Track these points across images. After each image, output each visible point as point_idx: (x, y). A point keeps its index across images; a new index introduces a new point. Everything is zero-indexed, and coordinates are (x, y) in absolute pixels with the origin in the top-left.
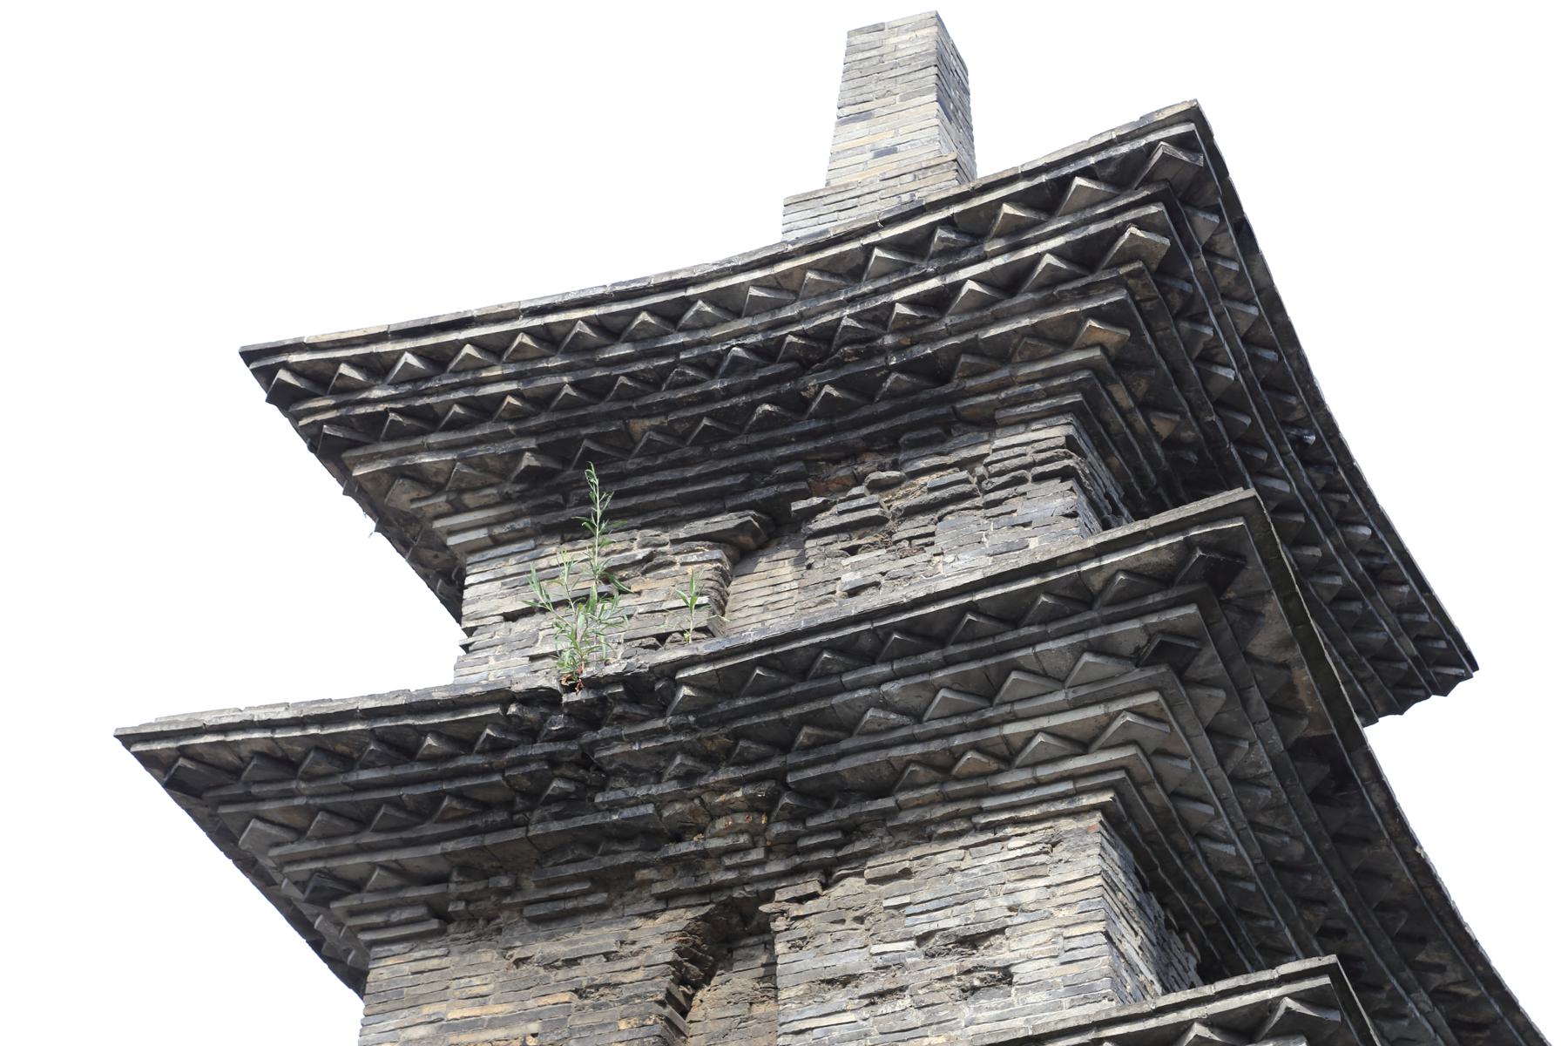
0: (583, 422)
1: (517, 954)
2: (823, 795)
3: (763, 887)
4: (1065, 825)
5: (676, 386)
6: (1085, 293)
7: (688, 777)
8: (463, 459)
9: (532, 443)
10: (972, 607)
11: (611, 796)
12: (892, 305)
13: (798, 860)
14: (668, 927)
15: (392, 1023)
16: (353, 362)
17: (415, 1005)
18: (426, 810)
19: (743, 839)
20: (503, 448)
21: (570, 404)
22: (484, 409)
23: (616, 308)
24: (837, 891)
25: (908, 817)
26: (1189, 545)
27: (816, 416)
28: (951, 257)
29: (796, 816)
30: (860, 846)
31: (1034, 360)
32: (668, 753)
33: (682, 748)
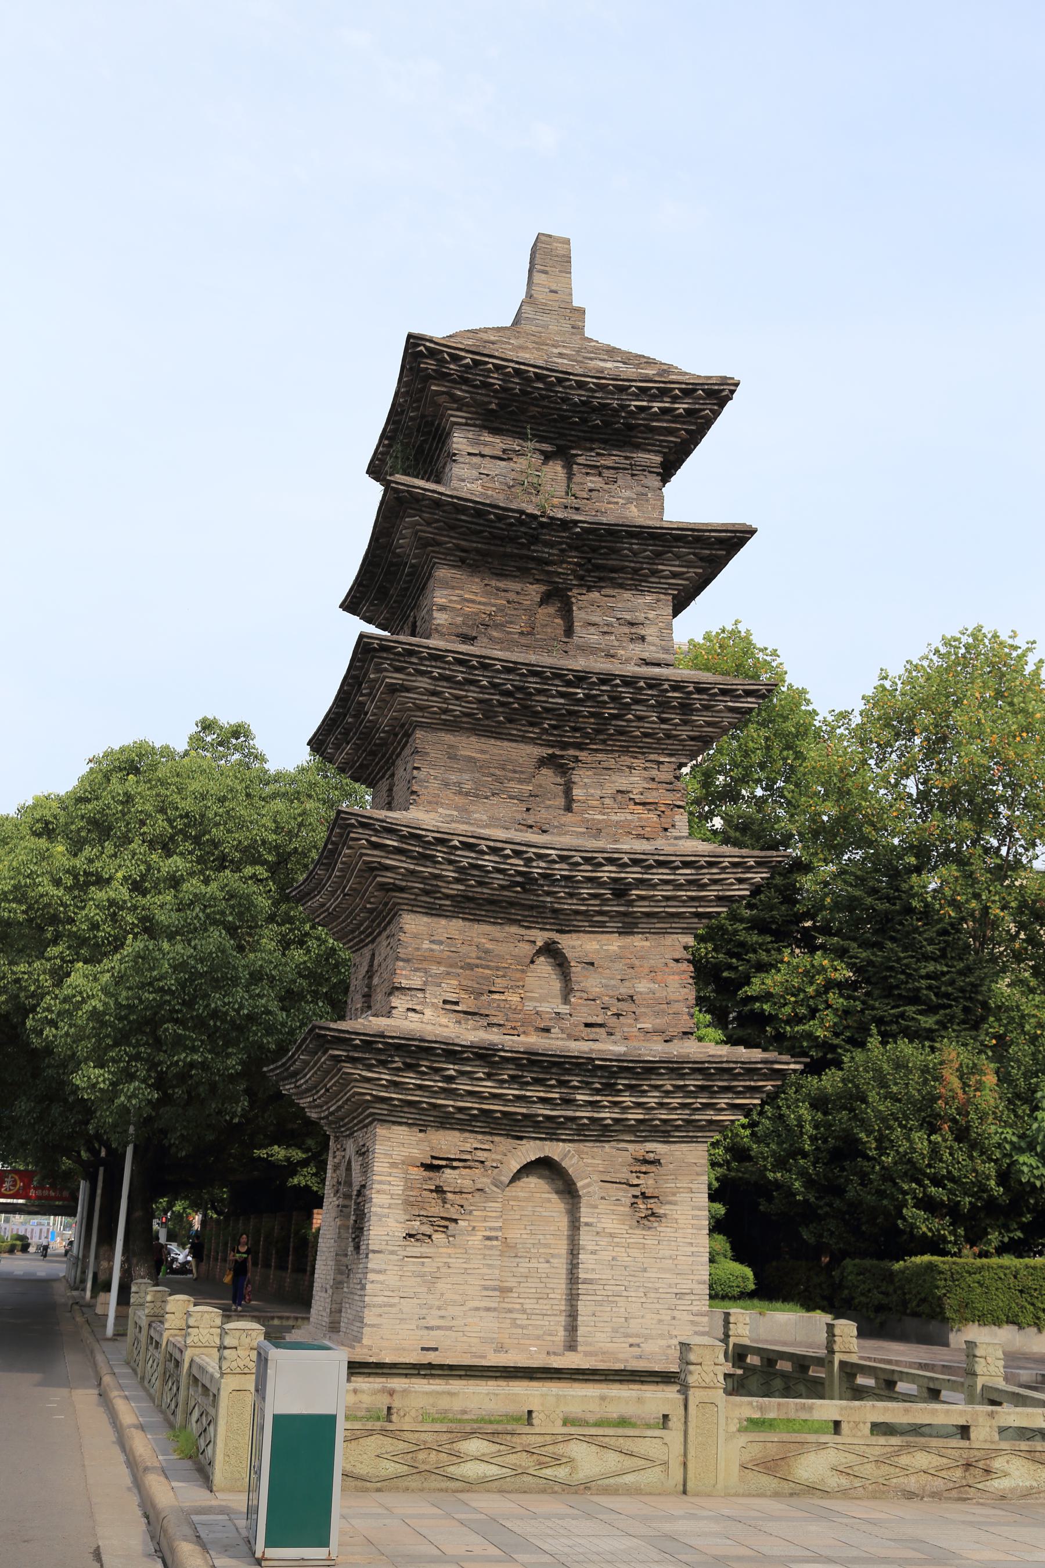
1: (486, 582)
2: (598, 568)
4: (662, 596)
5: (551, 402)
6: (684, 423)
7: (562, 551)
8: (471, 398)
11: (536, 548)
12: (630, 405)
15: (445, 592)
16: (449, 354)
17: (453, 588)
20: (486, 399)
21: (516, 395)
22: (486, 385)
23: (545, 372)
25: (620, 581)
26: (733, 537)
28: (653, 398)
29: (588, 571)
31: (660, 435)
32: (561, 543)
33: (566, 543)
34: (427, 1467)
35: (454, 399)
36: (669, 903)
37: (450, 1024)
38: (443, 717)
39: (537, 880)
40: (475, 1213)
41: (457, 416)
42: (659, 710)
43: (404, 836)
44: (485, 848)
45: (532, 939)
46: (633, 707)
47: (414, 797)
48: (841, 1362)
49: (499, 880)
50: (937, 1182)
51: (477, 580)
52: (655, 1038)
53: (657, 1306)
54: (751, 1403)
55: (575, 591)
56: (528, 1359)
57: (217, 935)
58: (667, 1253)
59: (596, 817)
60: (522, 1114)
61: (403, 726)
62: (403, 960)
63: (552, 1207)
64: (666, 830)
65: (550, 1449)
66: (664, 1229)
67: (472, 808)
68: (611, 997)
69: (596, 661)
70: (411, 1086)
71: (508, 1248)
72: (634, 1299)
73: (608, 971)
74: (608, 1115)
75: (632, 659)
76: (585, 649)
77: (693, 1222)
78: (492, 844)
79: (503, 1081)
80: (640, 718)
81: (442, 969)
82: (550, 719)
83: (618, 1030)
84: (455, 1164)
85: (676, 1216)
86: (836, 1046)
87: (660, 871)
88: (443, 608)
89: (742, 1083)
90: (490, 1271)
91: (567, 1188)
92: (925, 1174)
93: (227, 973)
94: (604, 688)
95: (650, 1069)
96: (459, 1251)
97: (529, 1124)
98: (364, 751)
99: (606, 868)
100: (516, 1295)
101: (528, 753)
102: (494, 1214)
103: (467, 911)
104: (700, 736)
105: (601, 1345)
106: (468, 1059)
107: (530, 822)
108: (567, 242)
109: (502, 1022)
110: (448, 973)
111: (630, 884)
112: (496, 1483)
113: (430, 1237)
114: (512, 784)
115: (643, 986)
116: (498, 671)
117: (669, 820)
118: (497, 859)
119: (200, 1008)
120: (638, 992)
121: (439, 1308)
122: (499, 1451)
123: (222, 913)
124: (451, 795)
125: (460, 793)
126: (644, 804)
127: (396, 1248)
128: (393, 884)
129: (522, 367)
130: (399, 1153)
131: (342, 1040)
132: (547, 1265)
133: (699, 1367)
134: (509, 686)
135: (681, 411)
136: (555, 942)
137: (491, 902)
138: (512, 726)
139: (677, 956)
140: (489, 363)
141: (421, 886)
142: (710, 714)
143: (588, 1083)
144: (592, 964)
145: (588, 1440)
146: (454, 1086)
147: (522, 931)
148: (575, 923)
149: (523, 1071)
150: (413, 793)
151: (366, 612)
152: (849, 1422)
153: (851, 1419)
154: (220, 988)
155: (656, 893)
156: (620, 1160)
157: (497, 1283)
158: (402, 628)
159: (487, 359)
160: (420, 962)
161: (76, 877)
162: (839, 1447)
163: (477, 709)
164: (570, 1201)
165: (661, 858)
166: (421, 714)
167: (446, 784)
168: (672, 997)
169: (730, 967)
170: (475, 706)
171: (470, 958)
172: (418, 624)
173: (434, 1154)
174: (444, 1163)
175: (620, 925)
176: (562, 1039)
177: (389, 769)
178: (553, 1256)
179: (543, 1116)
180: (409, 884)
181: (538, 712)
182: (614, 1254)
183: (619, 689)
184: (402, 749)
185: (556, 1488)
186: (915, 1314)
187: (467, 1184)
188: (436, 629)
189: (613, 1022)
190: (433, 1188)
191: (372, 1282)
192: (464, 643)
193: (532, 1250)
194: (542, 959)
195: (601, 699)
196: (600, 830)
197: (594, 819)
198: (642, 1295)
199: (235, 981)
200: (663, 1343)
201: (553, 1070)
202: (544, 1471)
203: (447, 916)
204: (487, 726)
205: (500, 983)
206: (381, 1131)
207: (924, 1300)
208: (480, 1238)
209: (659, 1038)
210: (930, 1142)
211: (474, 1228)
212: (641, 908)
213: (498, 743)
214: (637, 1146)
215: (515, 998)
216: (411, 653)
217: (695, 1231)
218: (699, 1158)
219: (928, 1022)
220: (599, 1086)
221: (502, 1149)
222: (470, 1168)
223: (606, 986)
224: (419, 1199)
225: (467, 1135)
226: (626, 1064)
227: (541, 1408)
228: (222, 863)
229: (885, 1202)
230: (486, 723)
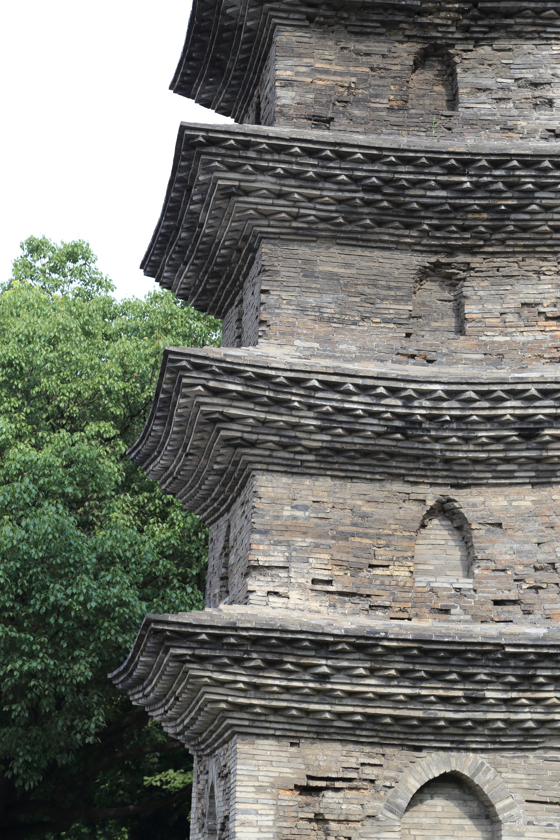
1: (342, 45)
2: (487, 13)
3: (450, 42)
13: (468, 35)
14: (409, 49)
15: (290, 63)
17: (300, 56)
19: (450, 22)
25: (517, 29)
29: (475, 19)
30: (493, 35)
37: (322, 609)
38: (294, 224)
39: (420, 423)
43: (249, 379)
44: (351, 388)
45: (421, 497)
46: (537, 195)
47: (264, 328)
49: (372, 426)
51: (330, 43)
55: (459, 47)
57: (51, 510)
59: (496, 339)
60: (418, 719)
61: (246, 239)
62: (260, 532)
67: (337, 337)
68: (526, 566)
69: (489, 138)
70: (275, 689)
73: (520, 533)
74: (528, 716)
75: (536, 131)
76: (476, 124)
78: (360, 381)
79: (391, 678)
80: (547, 209)
81: (309, 540)
82: (431, 218)
83: (536, 607)
84: (338, 784)
88: (288, 84)
91: (484, 812)
93: (68, 558)
94: (497, 173)
98: (206, 272)
99: (508, 404)
101: (403, 263)
103: (336, 466)
106: (343, 652)
107: (411, 351)
109: (387, 604)
110: (317, 546)
111: (540, 422)
116: (358, 161)
118: (368, 400)
119: (36, 604)
123: (61, 484)
124: (310, 323)
125: (321, 319)
128: (241, 438)
130: (267, 774)
131: (184, 636)
134: (374, 179)
136: (450, 500)
137: (366, 454)
138: (383, 230)
141: (276, 439)
143: (499, 676)
144: (500, 525)
146: (329, 686)
147: (408, 488)
148: (474, 475)
149: (414, 664)
150: (262, 322)
151: (201, 93)
154: (61, 577)
156: (550, 773)
158: (246, 112)
160: (283, 533)
163: (336, 211)
164: (489, 828)
166: (265, 222)
167: (303, 310)
170: (333, 208)
171: (344, 525)
172: (262, 105)
173: (310, 773)
174: (323, 784)
175: (533, 474)
176: (466, 621)
177: (237, 293)
180: (261, 437)
181: (416, 211)
183: (518, 173)
184: (249, 268)
187: (354, 810)
188: (281, 112)
190: (312, 816)
192: (317, 127)
194: (436, 522)
195: (494, 187)
196: (501, 356)
197: (493, 342)
199: (79, 565)
201: (453, 661)
203: (312, 475)
204: (350, 232)
205: (382, 556)
206: (242, 747)
213: (367, 253)
215: (401, 573)
216: (247, 145)
220: (513, 679)
221: (396, 763)
222: (357, 789)
223: (519, 552)
224: (295, 831)
225: (351, 747)
226: (545, 651)
228: (59, 420)
230: (349, 228)
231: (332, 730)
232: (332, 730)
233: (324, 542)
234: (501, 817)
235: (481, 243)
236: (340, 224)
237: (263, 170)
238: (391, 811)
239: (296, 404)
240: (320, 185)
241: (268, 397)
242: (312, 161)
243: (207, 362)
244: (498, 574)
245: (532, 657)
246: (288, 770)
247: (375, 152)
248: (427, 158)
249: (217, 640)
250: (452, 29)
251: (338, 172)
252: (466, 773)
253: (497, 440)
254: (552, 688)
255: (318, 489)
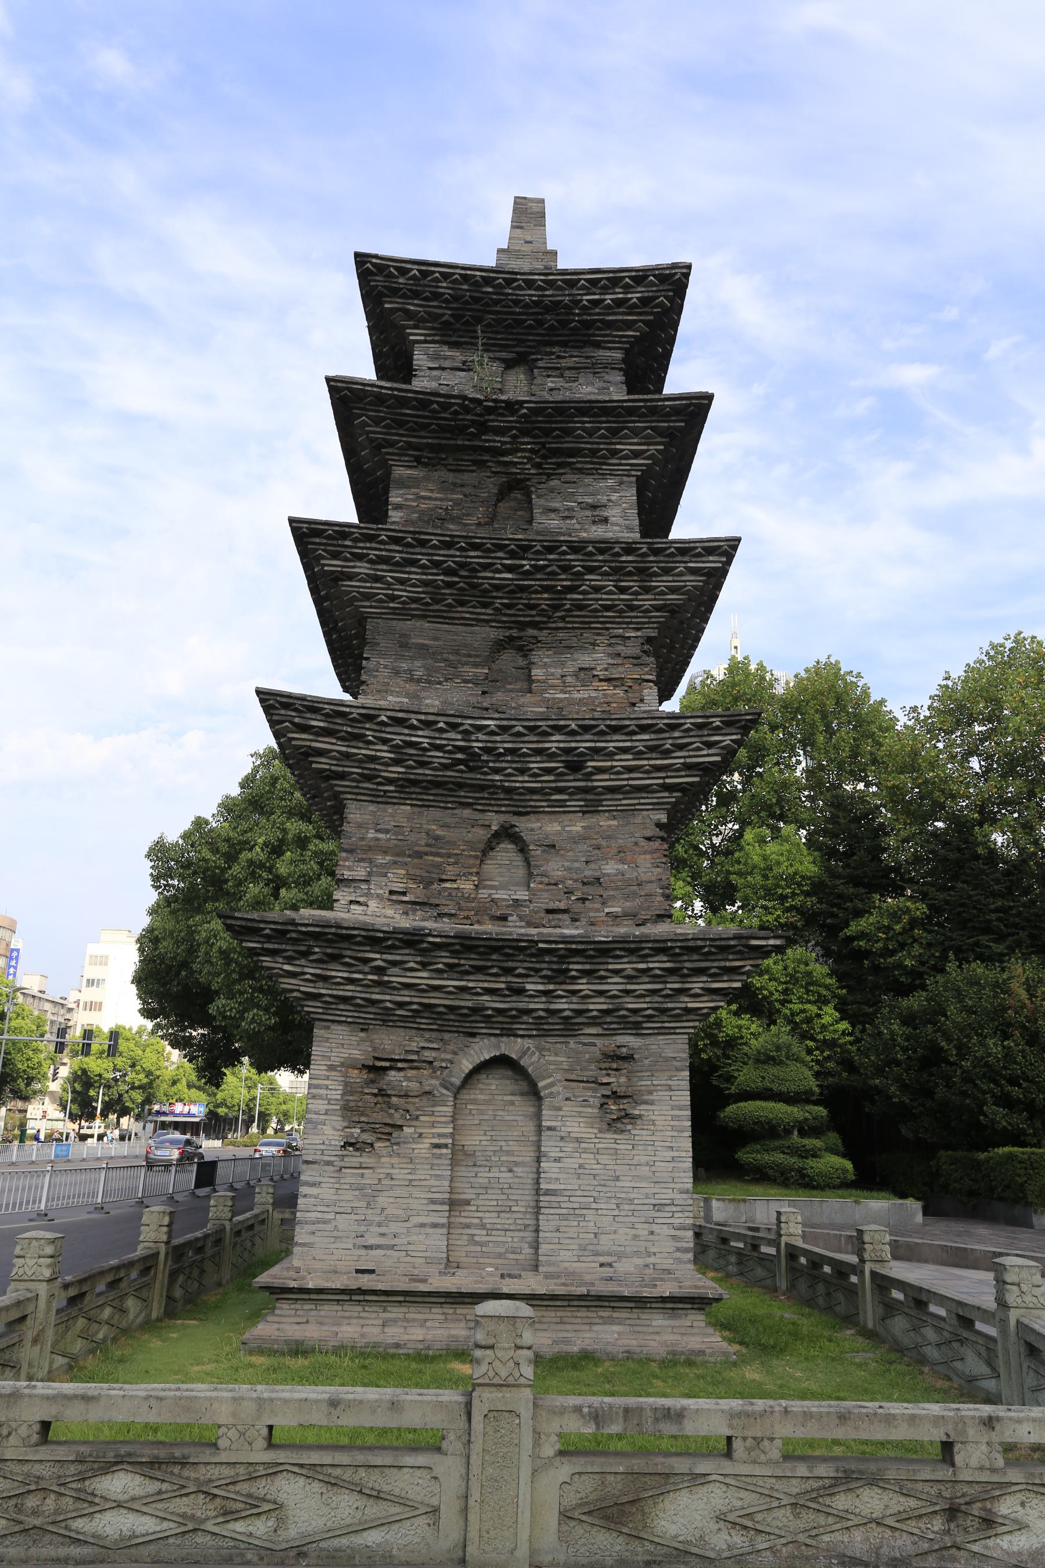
0: (468, 310)
2: (555, 452)
4: (625, 479)
5: (504, 306)
6: (640, 314)
7: (514, 437)
8: (425, 312)
9: (450, 312)
10: (622, 407)
15: (401, 492)
16: (395, 268)
17: (409, 487)
18: (424, 427)
22: (437, 296)
23: (492, 275)
24: (552, 483)
25: (579, 466)
27: (545, 329)
28: (605, 290)
29: (544, 457)
30: (561, 471)
32: (511, 429)
34: (38, 1522)
35: (409, 315)
36: (632, 775)
38: (391, 605)
40: (422, 1118)
41: (416, 335)
42: (615, 578)
43: (327, 715)
44: (415, 722)
45: (487, 823)
46: (586, 577)
48: (872, 1273)
50: (1013, 1081)
52: (626, 923)
53: (633, 1219)
54: (578, 1409)
56: (476, 1282)
58: (644, 1159)
62: (346, 851)
63: (516, 1112)
64: (634, 705)
65: (244, 1487)
66: (639, 1133)
67: (423, 694)
68: (576, 881)
71: (458, 1155)
72: (604, 1212)
73: (571, 853)
74: (566, 1006)
77: (672, 1123)
78: (423, 717)
80: (597, 589)
81: (388, 858)
83: (582, 915)
84: (399, 1065)
85: (653, 1118)
86: (923, 973)
87: (615, 738)
88: (398, 507)
89: (715, 964)
90: (438, 1183)
92: (1001, 1076)
94: (551, 557)
95: (605, 951)
96: (405, 1160)
97: (479, 1018)
99: (554, 738)
100: (474, 1208)
102: (443, 1119)
103: (414, 796)
104: (665, 606)
105: (567, 1265)
108: (542, 201)
109: (453, 912)
110: (395, 863)
111: (582, 754)
112: (152, 1547)
113: (372, 1145)
114: (466, 668)
115: (610, 868)
116: (434, 547)
117: (637, 695)
120: (604, 875)
121: (379, 1225)
122: (160, 1492)
125: (411, 680)
126: (608, 680)
127: (333, 1159)
128: (329, 770)
129: (469, 272)
130: (337, 1056)
132: (510, 1175)
133: (489, 1352)
135: (635, 300)
139: (649, 834)
140: (435, 272)
141: (359, 771)
142: (671, 578)
145: (310, 1472)
146: (386, 978)
147: (478, 816)
148: (532, 803)
149: (460, 959)
152: (745, 1439)
153: (749, 1433)
155: (615, 763)
156: (587, 1056)
157: (447, 1196)
159: (433, 269)
160: (364, 852)
161: (232, 846)
162: (728, 1480)
164: (536, 1103)
165: (613, 723)
166: (368, 604)
168: (644, 877)
169: (833, 915)
173: (376, 1055)
174: (387, 1064)
175: (582, 803)
178: (516, 1164)
179: (493, 1009)
180: (346, 769)
182: (581, 1161)
183: (568, 557)
185: (249, 1556)
186: (1001, 1199)
189: (578, 907)
190: (376, 1091)
191: (305, 1196)
193: (493, 1159)
195: (549, 569)
197: (555, 699)
198: (615, 1207)
200: (640, 1261)
201: (494, 957)
202: (232, 1526)
207: (1008, 1187)
208: (428, 1146)
209: (630, 922)
210: (1004, 1047)
211: (420, 1135)
212: (601, 781)
214: (606, 1041)
215: (467, 886)
217: (675, 1134)
218: (678, 1052)
219: (999, 948)
220: (549, 973)
221: (451, 1048)
223: (569, 869)
224: (360, 1104)
226: (574, 946)
227: (231, 1421)
229: (968, 1101)
230: (436, 607)
231: (396, 1018)
232: (396, 1018)
233: (401, 859)
234: (542, 1094)
235: (545, 619)
236: (427, 604)
237: (360, 557)
238: (446, 1088)
239: (370, 738)
240: (407, 569)
241: (346, 732)
242: (397, 548)
243: (292, 701)
244: (551, 887)
245: (562, 952)
246: (357, 1052)
247: (448, 539)
248: (492, 544)
249: (280, 934)
250: (528, 466)
251: (419, 557)
252: (514, 1056)
253: (548, 771)
254: (584, 981)
255: (400, 814)
